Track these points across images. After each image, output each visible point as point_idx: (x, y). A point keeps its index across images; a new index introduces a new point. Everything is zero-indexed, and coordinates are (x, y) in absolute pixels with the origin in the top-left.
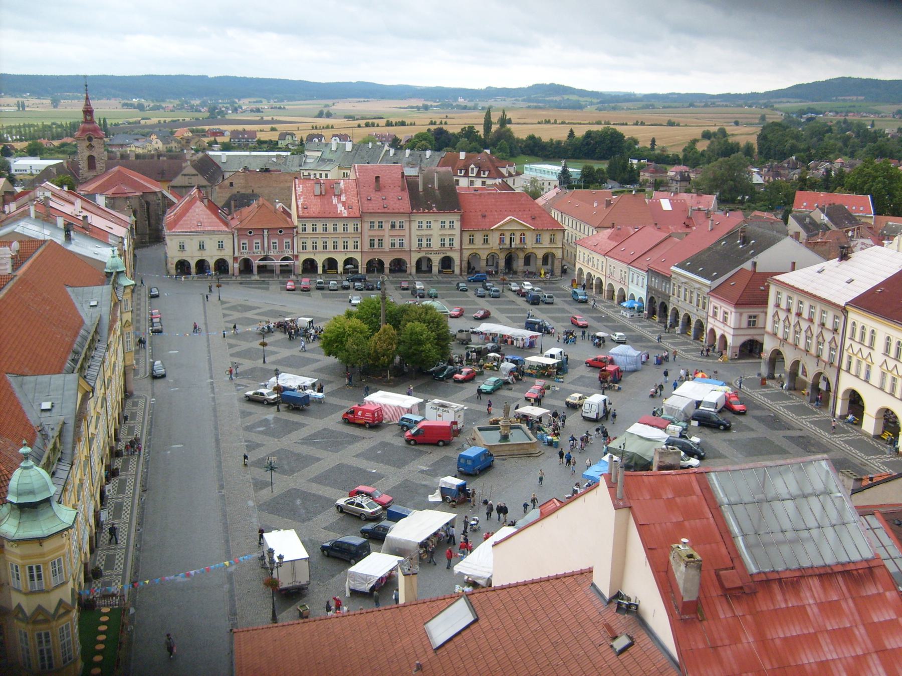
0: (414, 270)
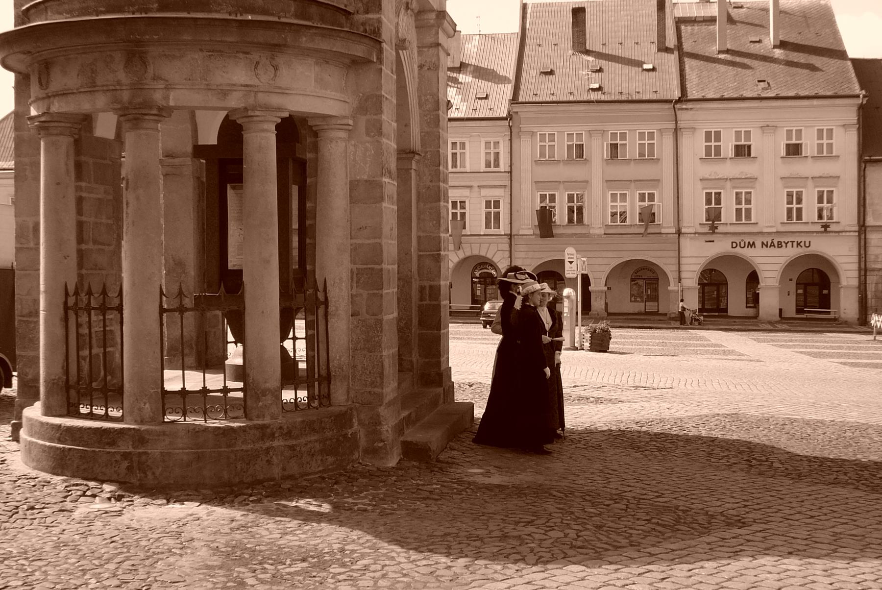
0: (692, 303)
